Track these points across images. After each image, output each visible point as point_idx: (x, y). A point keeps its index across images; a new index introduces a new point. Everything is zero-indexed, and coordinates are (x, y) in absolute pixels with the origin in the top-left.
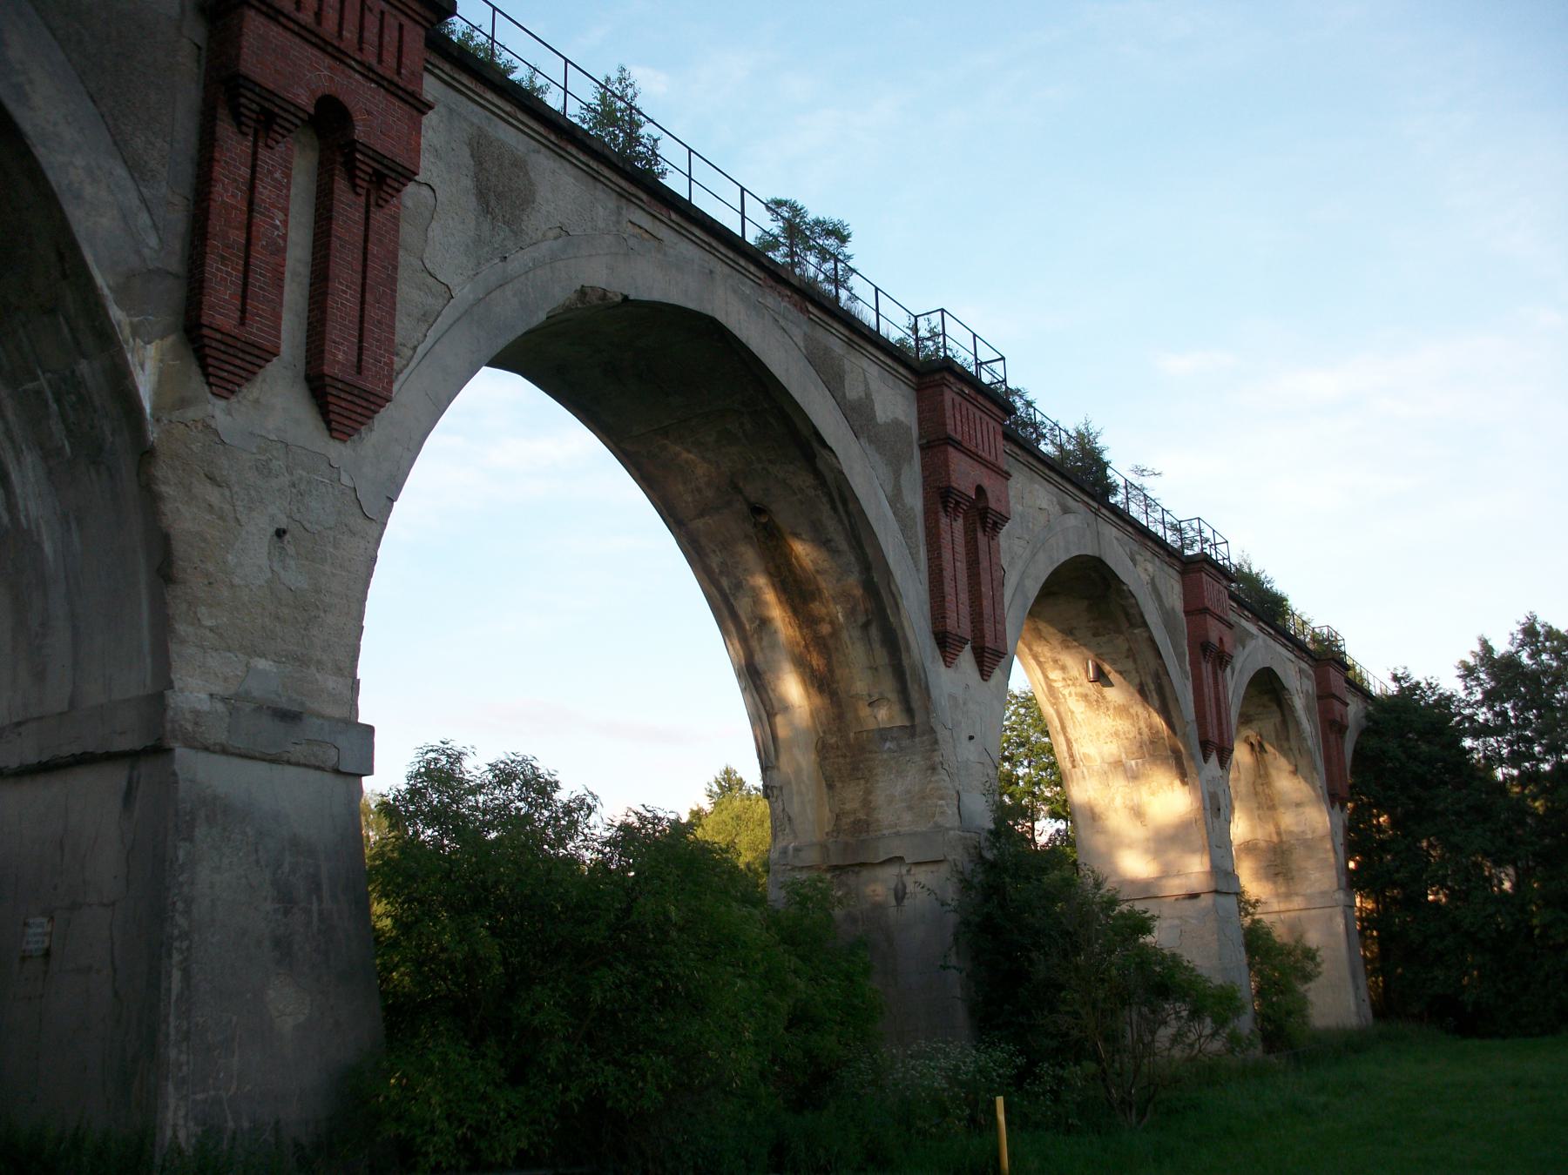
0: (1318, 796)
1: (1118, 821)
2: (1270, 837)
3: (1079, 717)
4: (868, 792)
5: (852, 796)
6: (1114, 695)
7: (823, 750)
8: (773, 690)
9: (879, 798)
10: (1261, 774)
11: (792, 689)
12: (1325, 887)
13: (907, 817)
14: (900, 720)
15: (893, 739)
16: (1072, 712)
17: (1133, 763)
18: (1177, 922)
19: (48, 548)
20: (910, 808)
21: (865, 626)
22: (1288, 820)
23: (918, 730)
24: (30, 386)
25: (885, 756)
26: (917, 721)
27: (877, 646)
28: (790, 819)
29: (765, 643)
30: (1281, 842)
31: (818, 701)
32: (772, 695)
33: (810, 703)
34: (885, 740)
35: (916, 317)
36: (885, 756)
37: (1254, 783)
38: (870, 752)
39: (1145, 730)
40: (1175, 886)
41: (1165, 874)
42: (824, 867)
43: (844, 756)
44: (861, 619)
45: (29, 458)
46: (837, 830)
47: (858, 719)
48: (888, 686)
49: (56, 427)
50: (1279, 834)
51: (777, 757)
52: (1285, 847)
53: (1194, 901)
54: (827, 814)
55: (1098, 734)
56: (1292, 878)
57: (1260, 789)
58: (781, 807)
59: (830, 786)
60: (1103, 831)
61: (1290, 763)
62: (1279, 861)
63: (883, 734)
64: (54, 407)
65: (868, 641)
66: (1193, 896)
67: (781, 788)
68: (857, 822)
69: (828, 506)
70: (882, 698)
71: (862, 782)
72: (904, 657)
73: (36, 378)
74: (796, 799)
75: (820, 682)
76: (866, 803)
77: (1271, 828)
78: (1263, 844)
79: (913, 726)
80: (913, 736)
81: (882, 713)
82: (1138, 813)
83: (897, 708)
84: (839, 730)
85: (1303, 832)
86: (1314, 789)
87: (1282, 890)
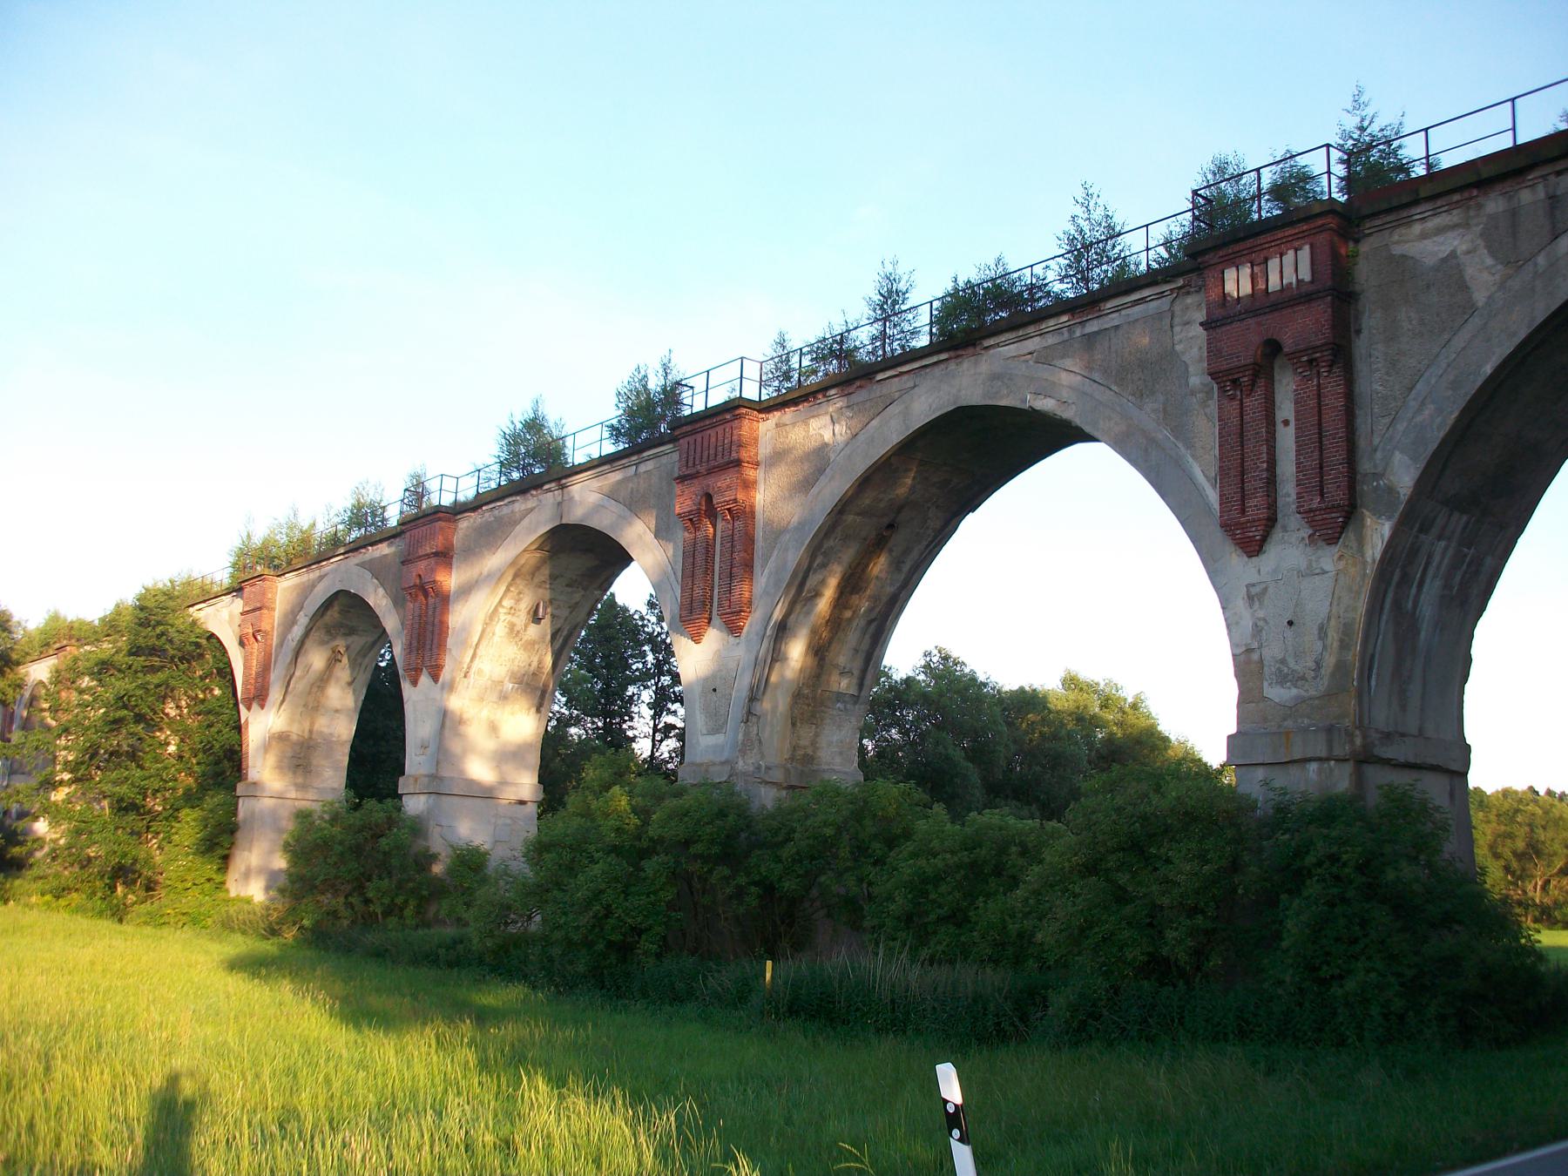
0: (356, 708)
1: (476, 732)
2: (303, 732)
3: (496, 639)
4: (817, 735)
5: (806, 733)
6: (533, 631)
7: (797, 696)
8: (786, 644)
9: (823, 741)
10: (323, 680)
11: (797, 651)
12: (336, 785)
13: (838, 760)
14: (853, 691)
15: (844, 702)
16: (494, 634)
17: (511, 685)
18: (509, 821)
19: (1423, 635)
20: (841, 753)
21: (870, 622)
22: (322, 724)
23: (861, 700)
24: (1466, 550)
25: (835, 713)
26: (863, 693)
27: (867, 636)
28: (760, 742)
29: (805, 609)
30: (310, 738)
31: (810, 660)
32: (783, 647)
33: (804, 662)
34: (838, 701)
35: (762, 363)
36: (835, 713)
37: (313, 684)
38: (826, 706)
39: (535, 664)
40: (510, 795)
41: (503, 783)
42: (785, 785)
43: (809, 705)
44: (873, 616)
45: (1438, 583)
46: (792, 758)
47: (828, 682)
48: (857, 665)
49: (1458, 578)
50: (311, 732)
51: (764, 693)
52: (312, 743)
53: (523, 807)
54: (787, 745)
55: (500, 656)
56: (310, 772)
57: (314, 690)
58: (755, 732)
59: (794, 724)
60: (459, 735)
61: (352, 674)
62: (302, 755)
63: (839, 696)
64: (1464, 567)
65: (864, 633)
66: (522, 803)
67: (759, 717)
68: (806, 755)
69: (596, 455)
70: (850, 672)
71: (814, 726)
72: (877, 650)
73: (1469, 548)
74: (768, 729)
75: (819, 652)
76: (813, 743)
77: (307, 726)
78: (294, 737)
79: (858, 696)
80: (855, 703)
81: (844, 683)
82: (493, 728)
83: (855, 681)
84: (814, 686)
85: (331, 734)
86: (356, 702)
87: (300, 780)
